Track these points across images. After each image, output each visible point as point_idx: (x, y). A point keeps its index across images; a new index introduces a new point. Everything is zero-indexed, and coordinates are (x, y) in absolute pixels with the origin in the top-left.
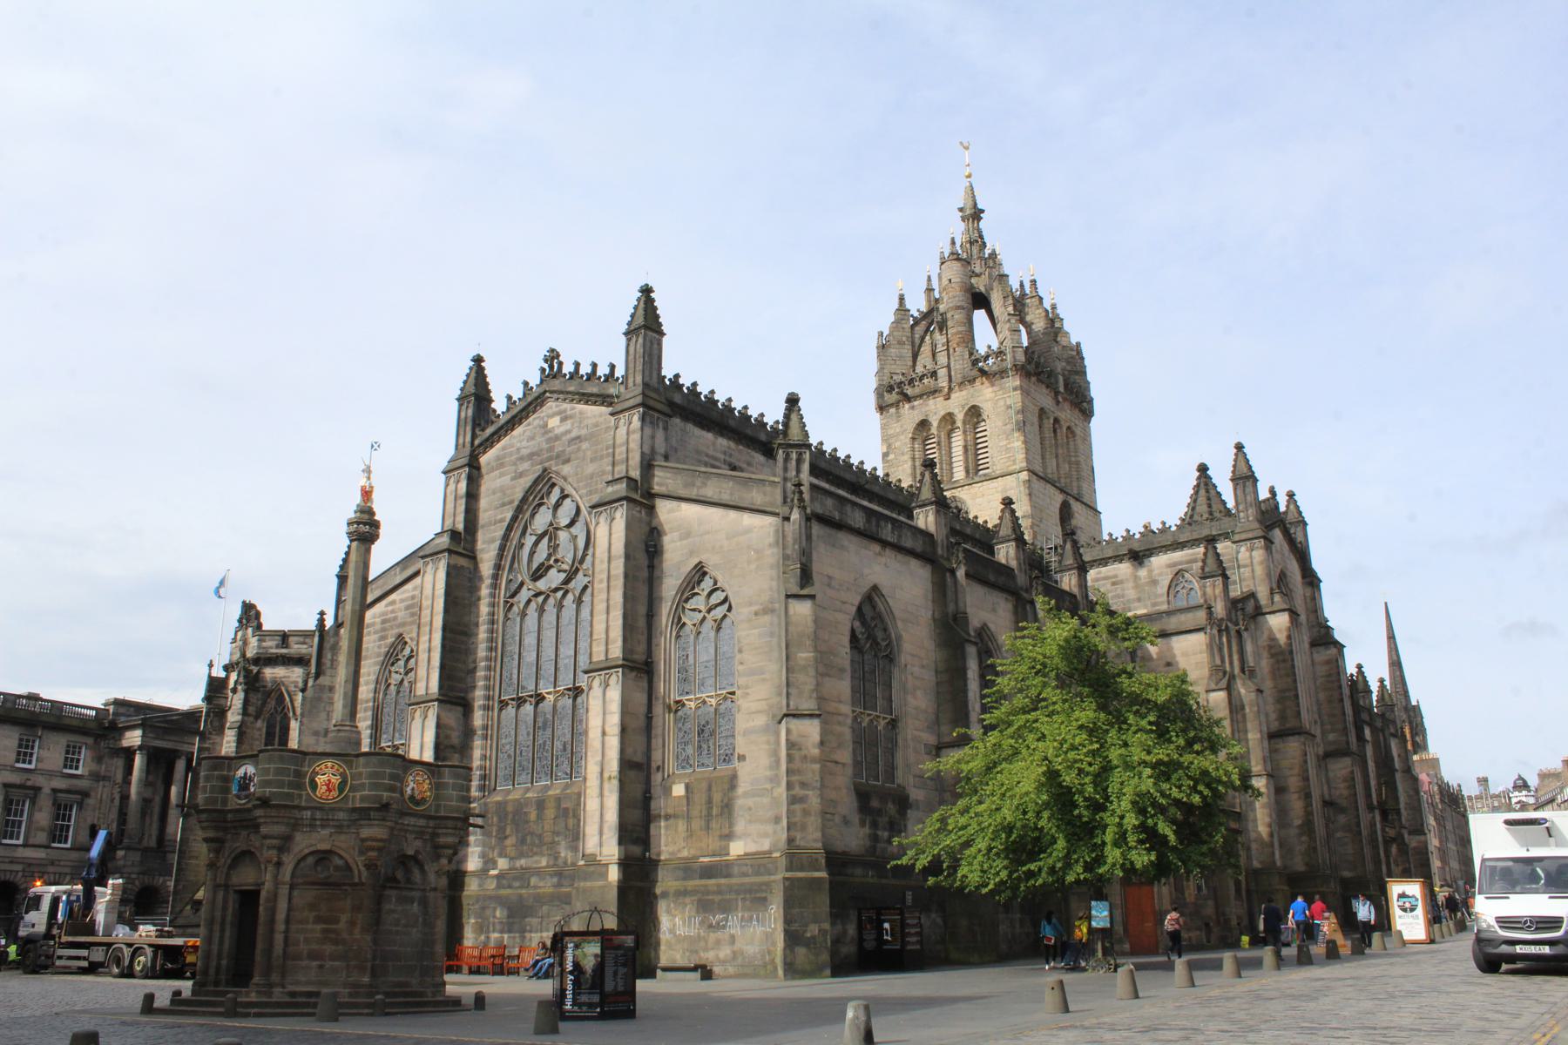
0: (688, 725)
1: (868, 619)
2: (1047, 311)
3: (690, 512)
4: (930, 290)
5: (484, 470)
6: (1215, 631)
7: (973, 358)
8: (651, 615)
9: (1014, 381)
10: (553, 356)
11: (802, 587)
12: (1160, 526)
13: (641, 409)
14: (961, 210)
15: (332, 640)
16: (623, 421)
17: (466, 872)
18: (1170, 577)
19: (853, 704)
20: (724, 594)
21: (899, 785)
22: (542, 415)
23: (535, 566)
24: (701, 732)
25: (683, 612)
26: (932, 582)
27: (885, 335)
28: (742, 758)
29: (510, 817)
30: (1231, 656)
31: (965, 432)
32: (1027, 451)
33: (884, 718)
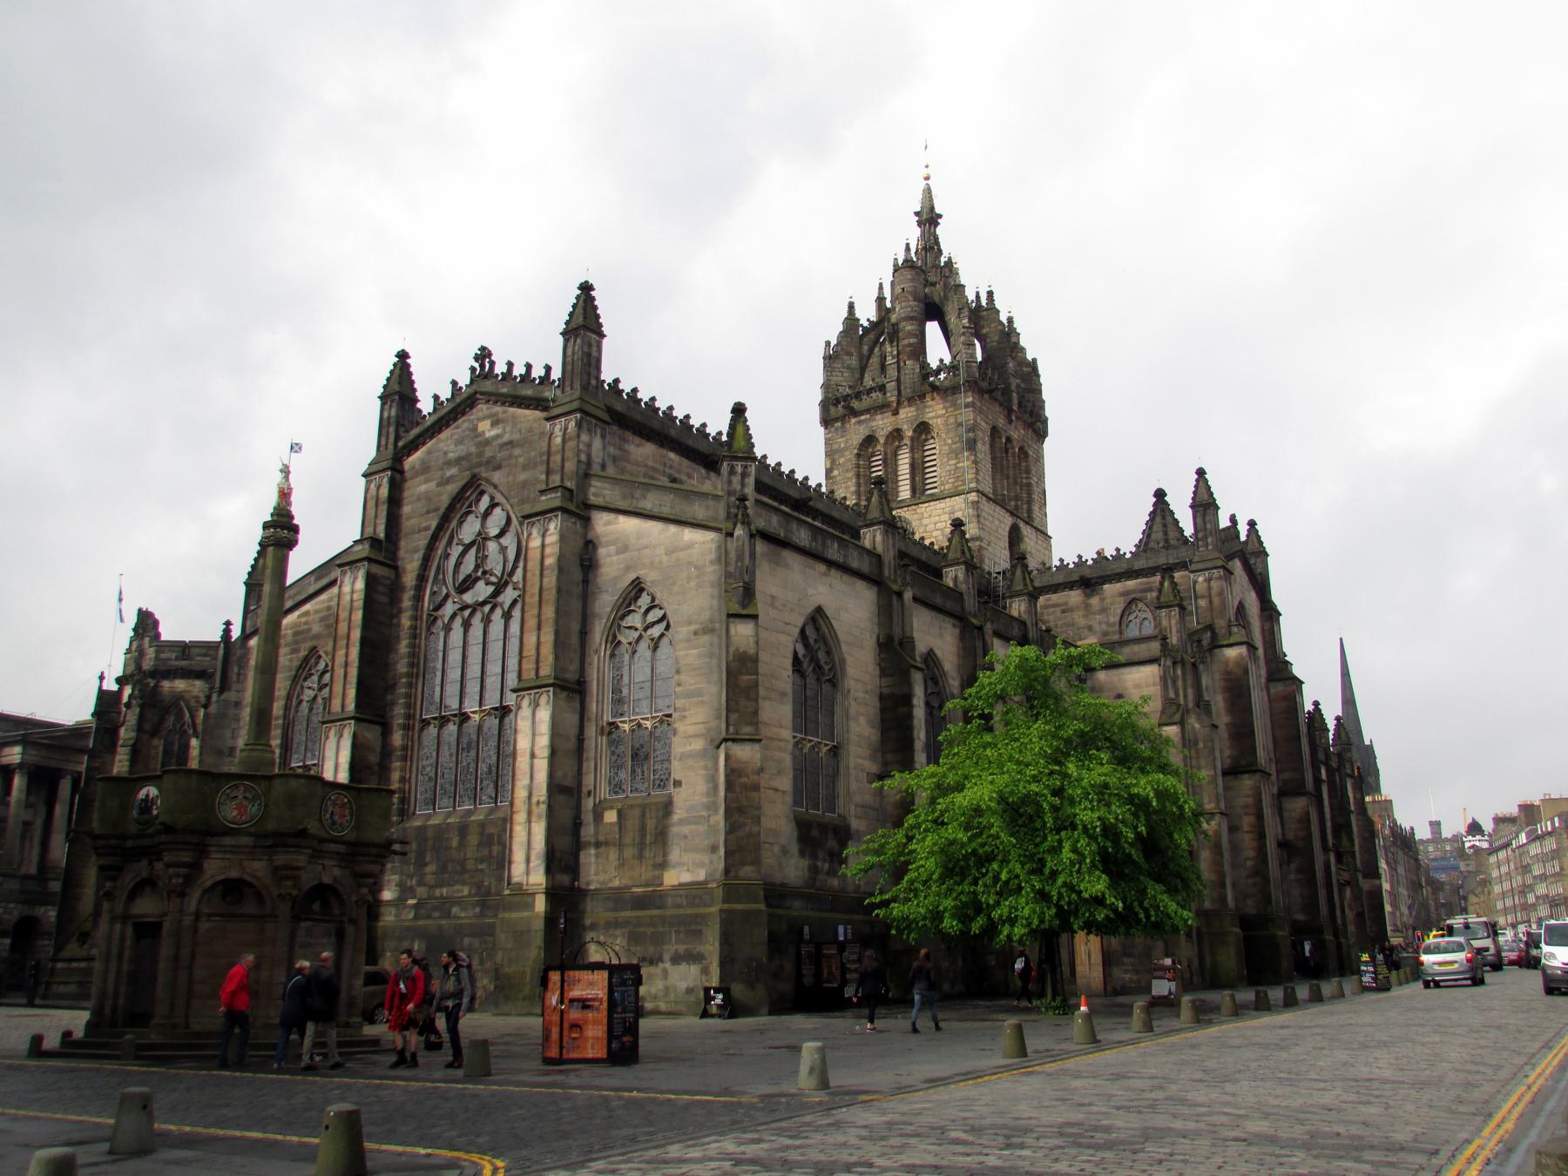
0: (621, 748)
1: (811, 641)
4: (880, 300)
5: (407, 475)
6: (1169, 663)
8: (584, 633)
10: (484, 355)
11: (744, 606)
12: (1114, 553)
13: (578, 415)
14: (917, 214)
15: (239, 652)
16: (558, 427)
17: (381, 901)
18: (1122, 606)
19: (795, 729)
20: (662, 612)
21: (839, 815)
22: (472, 417)
23: (461, 577)
24: (635, 756)
25: (619, 630)
26: (879, 607)
27: (832, 345)
28: (678, 784)
29: (430, 843)
30: (1185, 690)
33: (826, 745)
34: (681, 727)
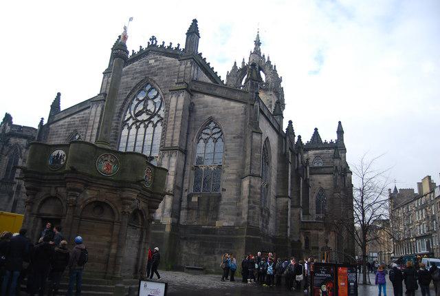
3: (208, 98)
10: (153, 38)
23: (137, 111)
26: (278, 141)
34: (226, 170)
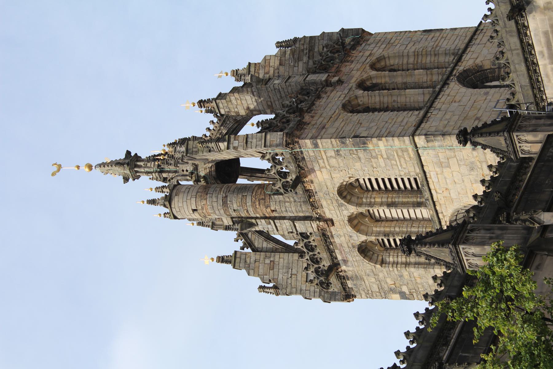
2: (235, 90)
7: (282, 191)
9: (307, 144)
14: (126, 180)
27: (263, 284)
31: (371, 205)
32: (390, 134)
